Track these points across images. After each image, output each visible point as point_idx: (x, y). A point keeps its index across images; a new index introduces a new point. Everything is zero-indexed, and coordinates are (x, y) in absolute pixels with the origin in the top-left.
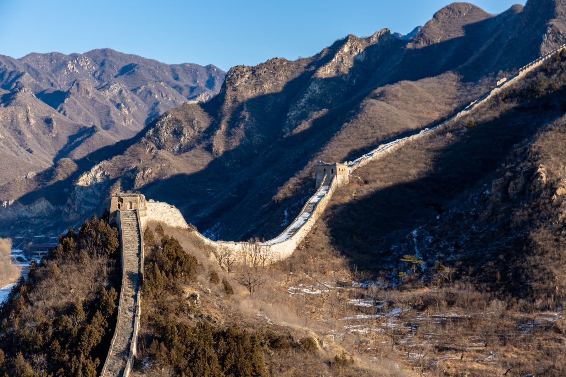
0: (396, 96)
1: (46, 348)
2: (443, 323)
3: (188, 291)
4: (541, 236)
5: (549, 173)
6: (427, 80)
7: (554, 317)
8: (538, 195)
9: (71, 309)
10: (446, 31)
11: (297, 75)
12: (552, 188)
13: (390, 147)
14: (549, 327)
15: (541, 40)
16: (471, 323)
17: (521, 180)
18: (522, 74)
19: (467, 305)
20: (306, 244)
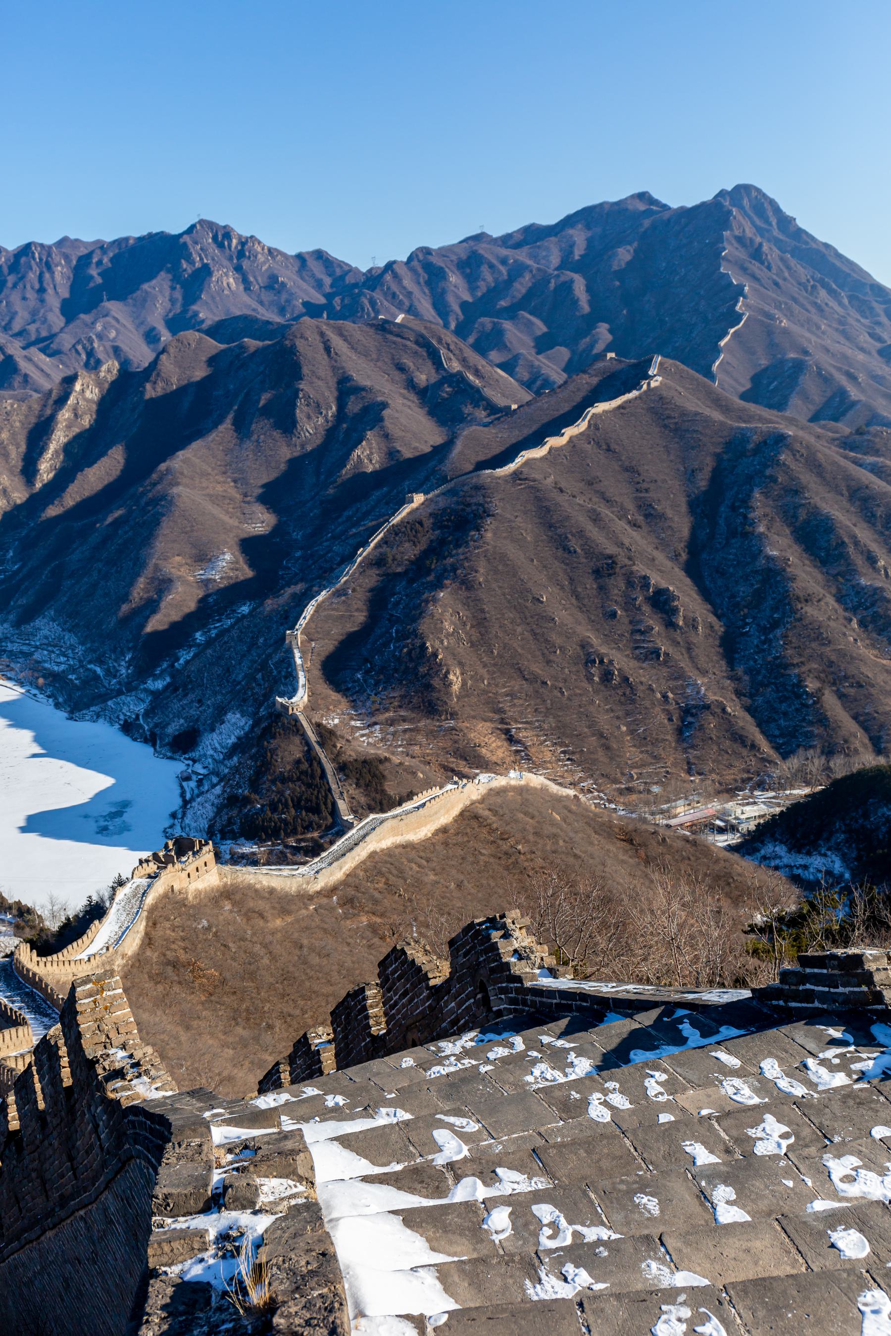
0: (182, 474)
1: (299, 779)
2: (405, 731)
3: (339, 745)
4: (436, 682)
5: (432, 646)
6: (195, 445)
7: (452, 723)
8: (428, 661)
9: (298, 762)
10: (180, 367)
11: (33, 420)
12: (435, 655)
13: (310, 610)
14: (453, 729)
15: (295, 405)
16: (416, 730)
17: (418, 650)
18: (372, 545)
19: (411, 721)
20: (312, 694)
